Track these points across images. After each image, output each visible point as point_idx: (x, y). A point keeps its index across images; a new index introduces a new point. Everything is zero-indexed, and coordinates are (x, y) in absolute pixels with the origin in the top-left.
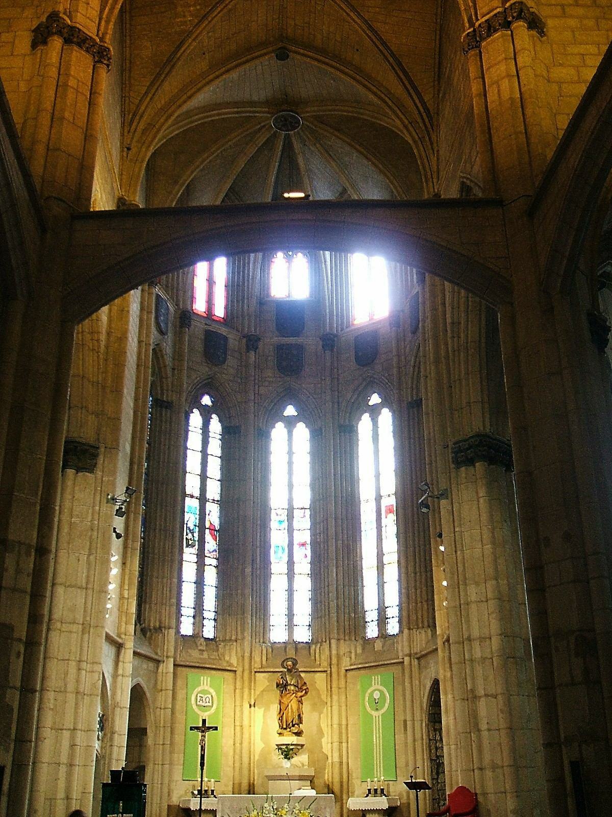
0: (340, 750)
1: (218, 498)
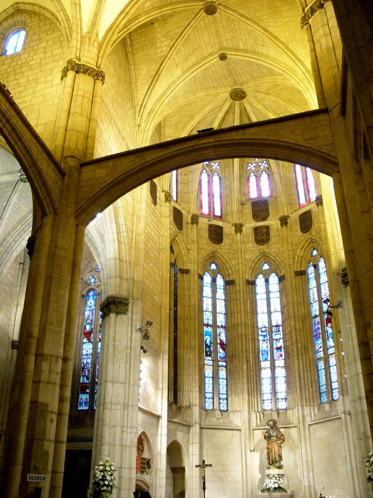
0: (308, 478)
1: (224, 324)
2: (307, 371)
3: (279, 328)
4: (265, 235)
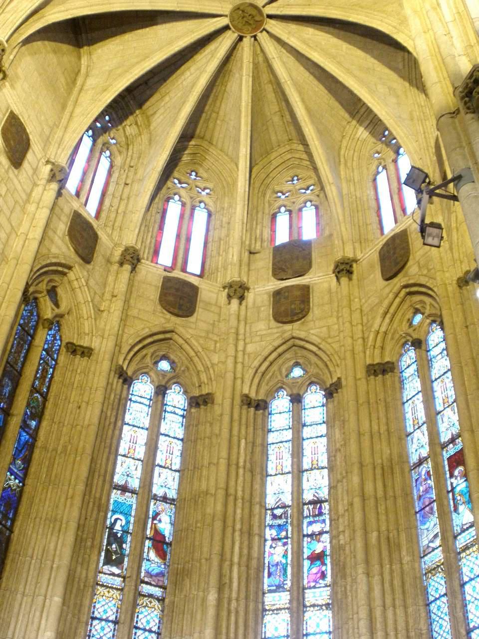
2: (394, 606)
3: (320, 508)
4: (298, 302)
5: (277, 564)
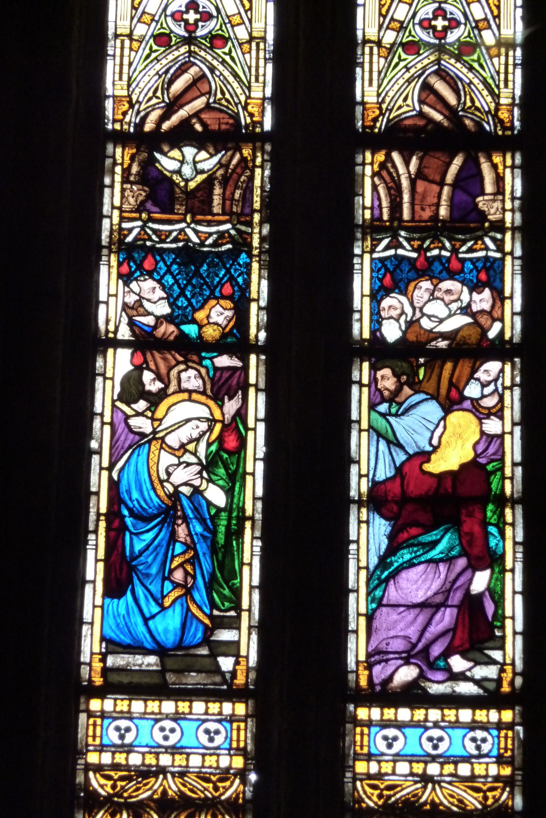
3: (469, 181)
5: (170, 511)
